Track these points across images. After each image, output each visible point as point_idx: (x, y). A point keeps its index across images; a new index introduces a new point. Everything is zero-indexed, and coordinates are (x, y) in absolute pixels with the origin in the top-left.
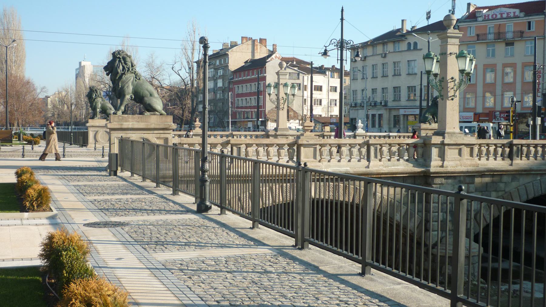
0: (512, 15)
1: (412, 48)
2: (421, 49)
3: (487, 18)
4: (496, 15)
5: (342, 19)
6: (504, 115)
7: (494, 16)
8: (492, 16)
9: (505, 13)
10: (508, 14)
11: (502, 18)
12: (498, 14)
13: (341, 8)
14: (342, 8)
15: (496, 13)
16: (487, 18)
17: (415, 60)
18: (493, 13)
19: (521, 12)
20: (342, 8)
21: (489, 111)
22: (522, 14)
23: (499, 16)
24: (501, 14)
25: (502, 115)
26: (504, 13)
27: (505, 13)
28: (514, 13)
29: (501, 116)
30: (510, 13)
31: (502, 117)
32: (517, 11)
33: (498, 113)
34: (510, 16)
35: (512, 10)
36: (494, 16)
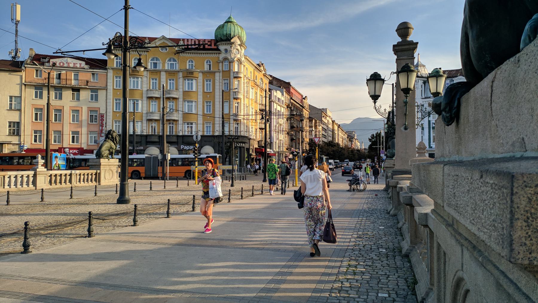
0: (78, 66)
4: (63, 64)
6: (73, 151)
7: (62, 64)
8: (60, 63)
9: (72, 63)
10: (74, 64)
12: (65, 63)
15: (63, 62)
18: (60, 61)
21: (59, 148)
25: (71, 151)
26: (71, 63)
27: (72, 63)
29: (70, 152)
30: (77, 64)
31: (71, 153)
32: (83, 63)
33: (68, 149)
34: (77, 66)
35: (79, 62)
36: (62, 64)
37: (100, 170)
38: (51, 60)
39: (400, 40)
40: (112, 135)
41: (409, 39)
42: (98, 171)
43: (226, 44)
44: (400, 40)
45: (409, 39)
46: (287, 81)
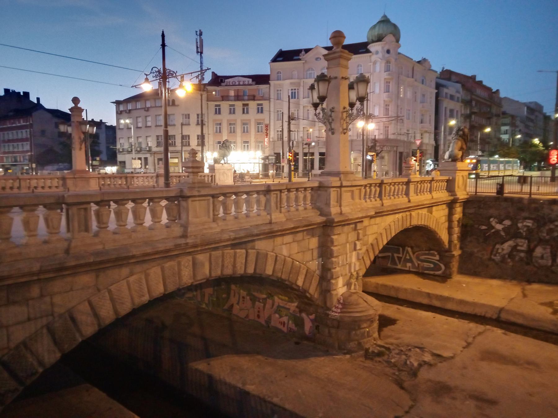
1: (171, 104)
2: (178, 106)
3: (228, 84)
4: (235, 83)
5: (163, 45)
7: (234, 83)
8: (232, 83)
11: (239, 85)
12: (236, 81)
13: (162, 33)
14: (163, 32)
16: (228, 84)
17: (174, 114)
18: (233, 81)
19: (253, 81)
20: (163, 32)
22: (254, 83)
23: (237, 83)
24: (239, 82)
28: (248, 81)
32: (250, 80)
35: (247, 79)
36: (234, 83)
37: (214, 173)
38: (226, 80)
39: (73, 105)
40: (226, 144)
41: (79, 105)
42: (214, 174)
43: (377, 45)
44: (73, 105)
45: (79, 105)
46: (469, 74)
